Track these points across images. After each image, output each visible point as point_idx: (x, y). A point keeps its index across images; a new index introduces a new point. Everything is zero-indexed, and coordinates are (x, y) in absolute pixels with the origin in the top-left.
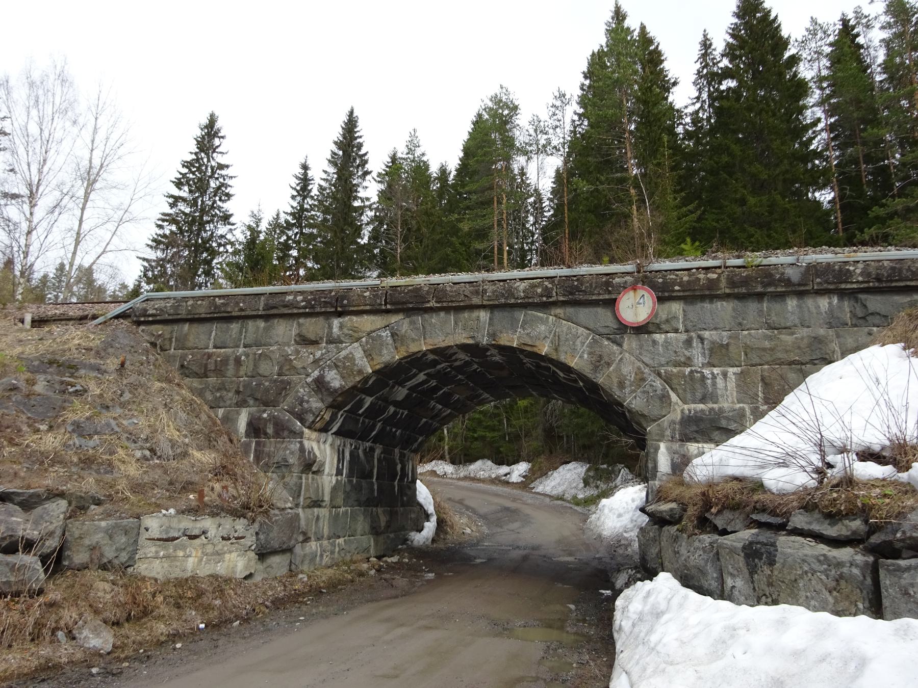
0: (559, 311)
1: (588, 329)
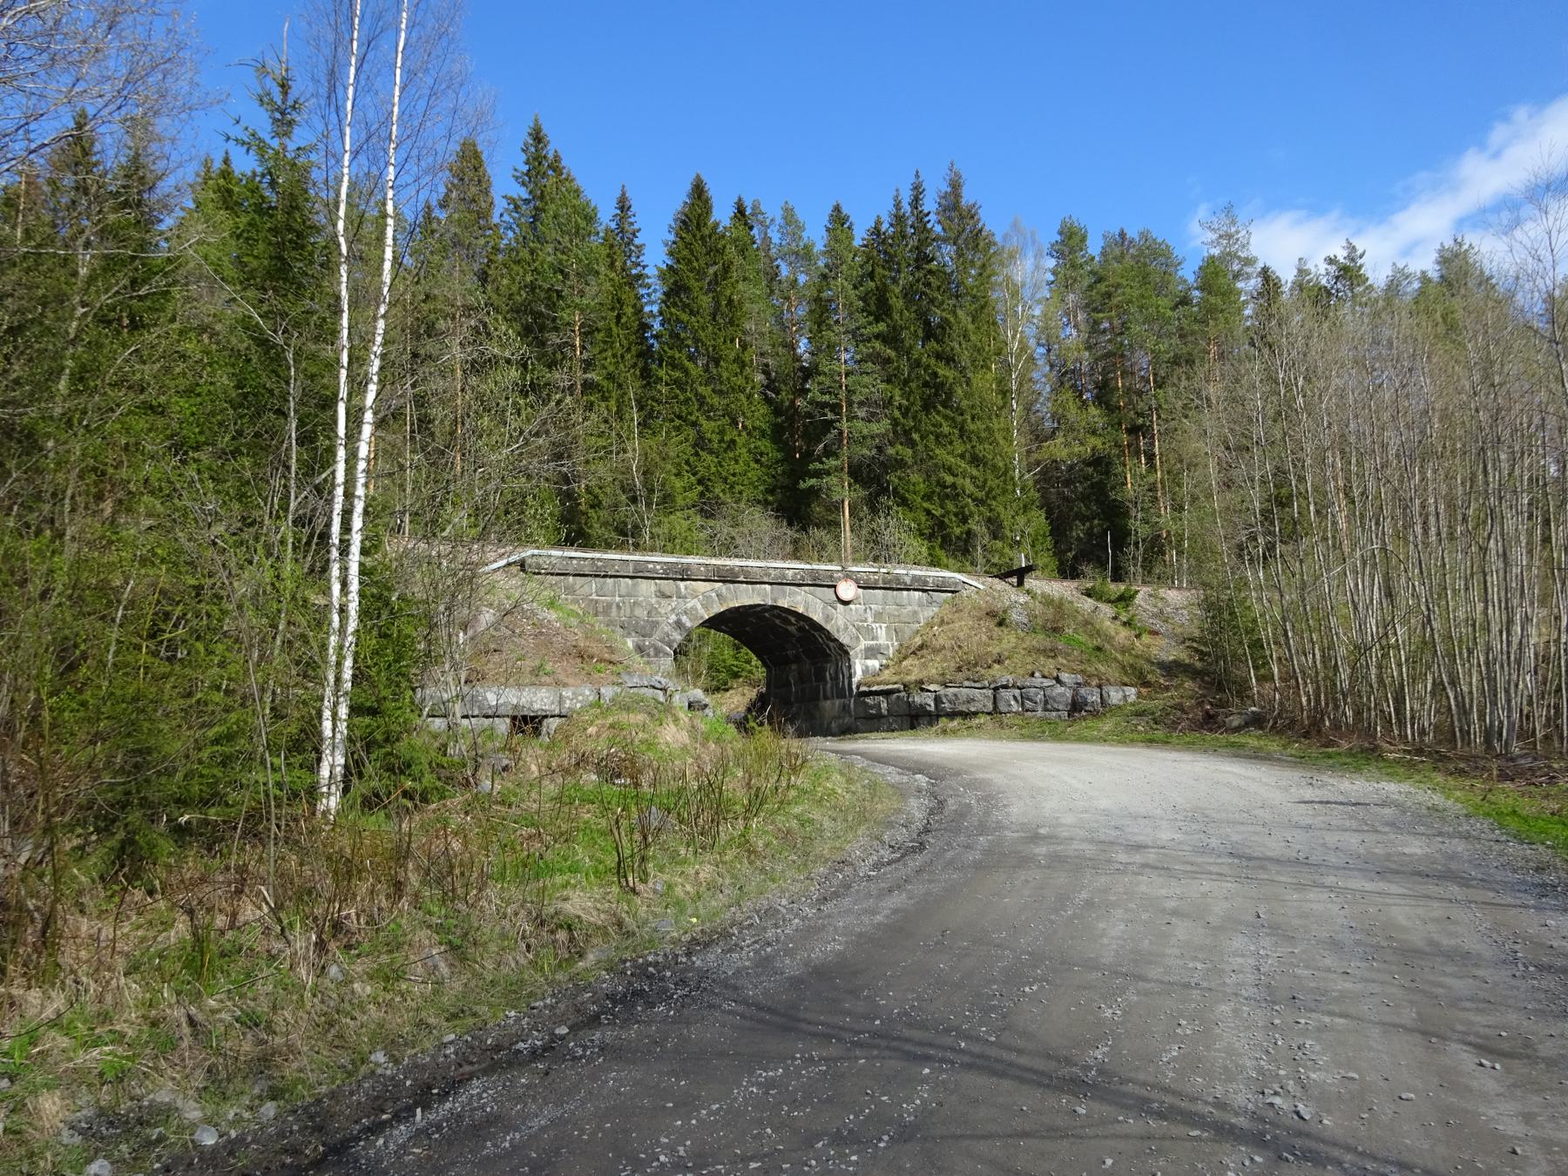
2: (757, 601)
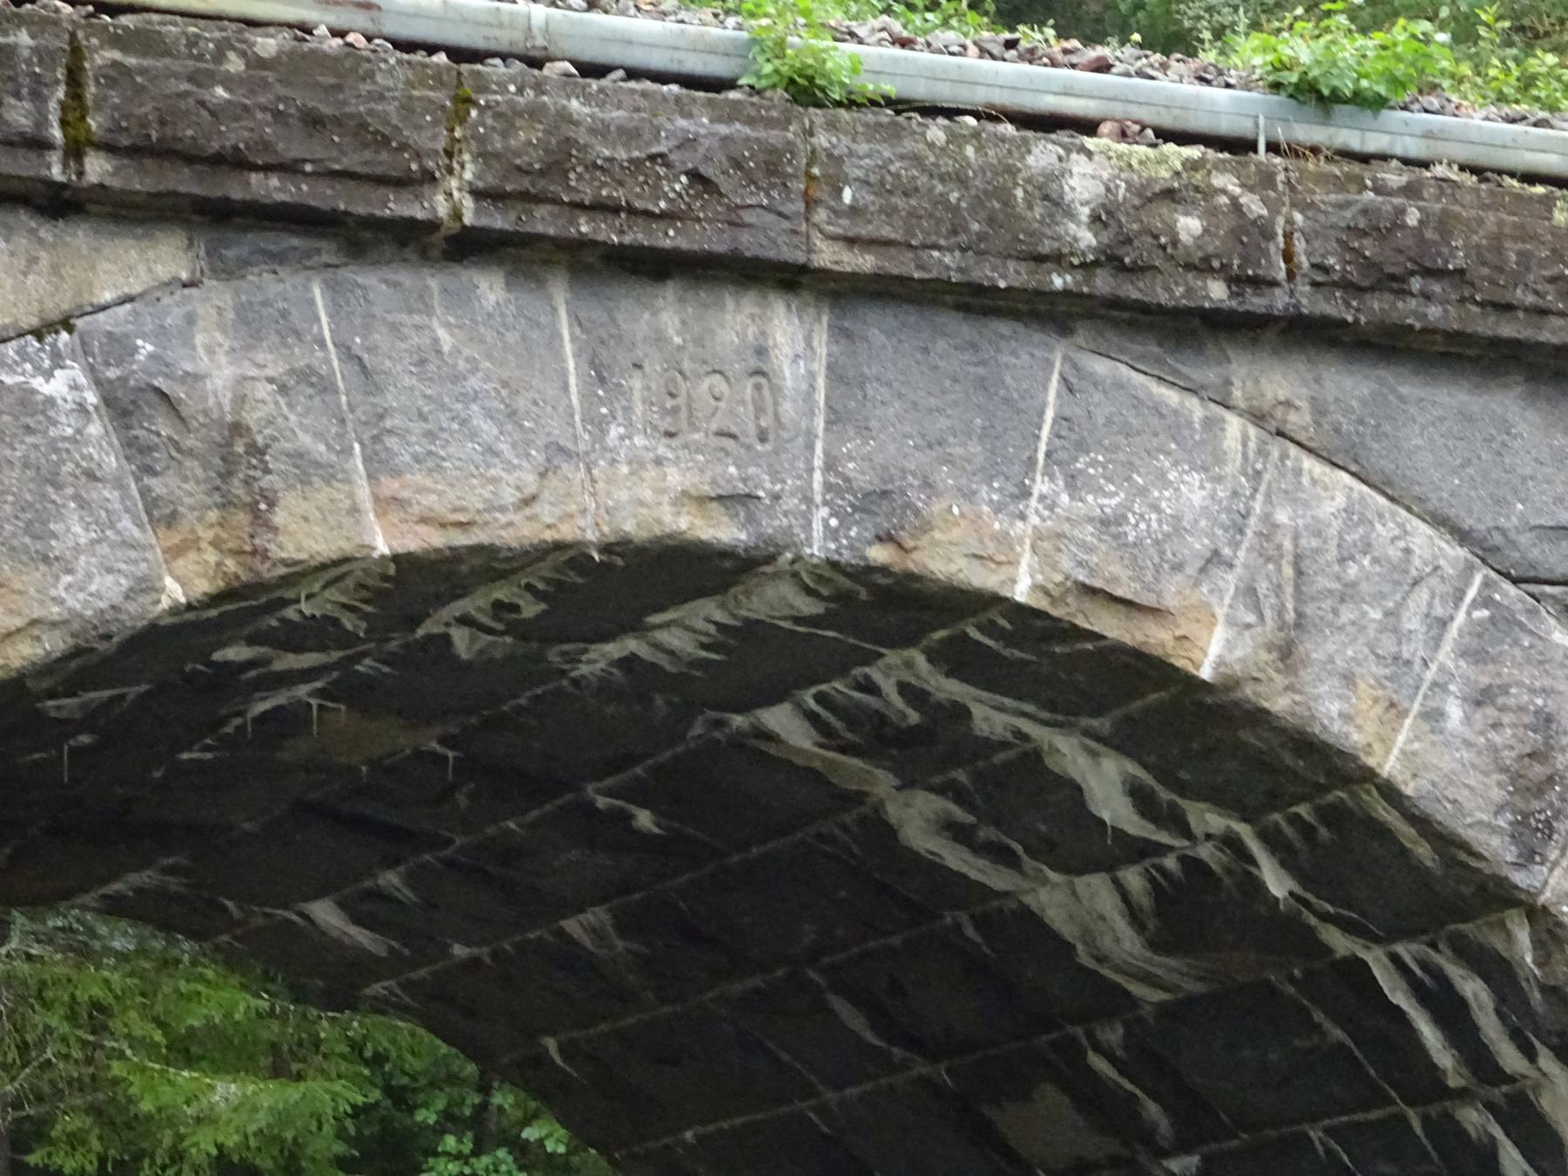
0: (1280, 381)
1: (1462, 536)
2: (638, 490)
